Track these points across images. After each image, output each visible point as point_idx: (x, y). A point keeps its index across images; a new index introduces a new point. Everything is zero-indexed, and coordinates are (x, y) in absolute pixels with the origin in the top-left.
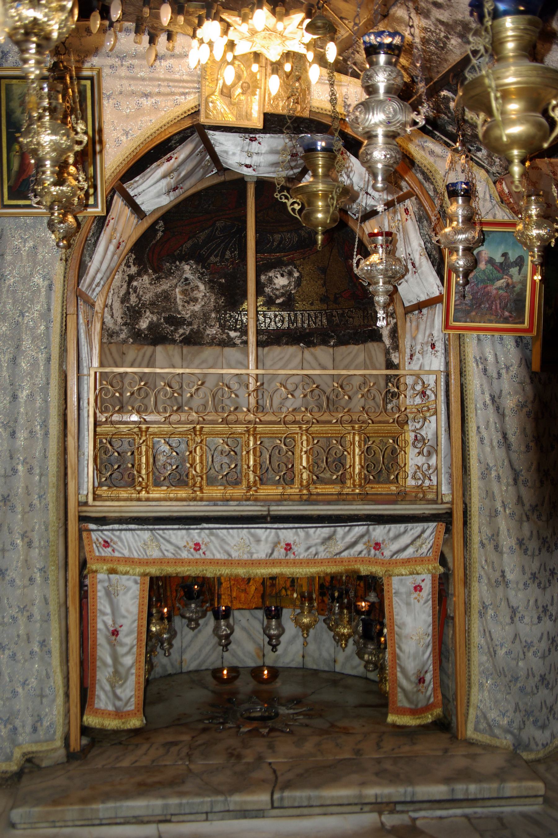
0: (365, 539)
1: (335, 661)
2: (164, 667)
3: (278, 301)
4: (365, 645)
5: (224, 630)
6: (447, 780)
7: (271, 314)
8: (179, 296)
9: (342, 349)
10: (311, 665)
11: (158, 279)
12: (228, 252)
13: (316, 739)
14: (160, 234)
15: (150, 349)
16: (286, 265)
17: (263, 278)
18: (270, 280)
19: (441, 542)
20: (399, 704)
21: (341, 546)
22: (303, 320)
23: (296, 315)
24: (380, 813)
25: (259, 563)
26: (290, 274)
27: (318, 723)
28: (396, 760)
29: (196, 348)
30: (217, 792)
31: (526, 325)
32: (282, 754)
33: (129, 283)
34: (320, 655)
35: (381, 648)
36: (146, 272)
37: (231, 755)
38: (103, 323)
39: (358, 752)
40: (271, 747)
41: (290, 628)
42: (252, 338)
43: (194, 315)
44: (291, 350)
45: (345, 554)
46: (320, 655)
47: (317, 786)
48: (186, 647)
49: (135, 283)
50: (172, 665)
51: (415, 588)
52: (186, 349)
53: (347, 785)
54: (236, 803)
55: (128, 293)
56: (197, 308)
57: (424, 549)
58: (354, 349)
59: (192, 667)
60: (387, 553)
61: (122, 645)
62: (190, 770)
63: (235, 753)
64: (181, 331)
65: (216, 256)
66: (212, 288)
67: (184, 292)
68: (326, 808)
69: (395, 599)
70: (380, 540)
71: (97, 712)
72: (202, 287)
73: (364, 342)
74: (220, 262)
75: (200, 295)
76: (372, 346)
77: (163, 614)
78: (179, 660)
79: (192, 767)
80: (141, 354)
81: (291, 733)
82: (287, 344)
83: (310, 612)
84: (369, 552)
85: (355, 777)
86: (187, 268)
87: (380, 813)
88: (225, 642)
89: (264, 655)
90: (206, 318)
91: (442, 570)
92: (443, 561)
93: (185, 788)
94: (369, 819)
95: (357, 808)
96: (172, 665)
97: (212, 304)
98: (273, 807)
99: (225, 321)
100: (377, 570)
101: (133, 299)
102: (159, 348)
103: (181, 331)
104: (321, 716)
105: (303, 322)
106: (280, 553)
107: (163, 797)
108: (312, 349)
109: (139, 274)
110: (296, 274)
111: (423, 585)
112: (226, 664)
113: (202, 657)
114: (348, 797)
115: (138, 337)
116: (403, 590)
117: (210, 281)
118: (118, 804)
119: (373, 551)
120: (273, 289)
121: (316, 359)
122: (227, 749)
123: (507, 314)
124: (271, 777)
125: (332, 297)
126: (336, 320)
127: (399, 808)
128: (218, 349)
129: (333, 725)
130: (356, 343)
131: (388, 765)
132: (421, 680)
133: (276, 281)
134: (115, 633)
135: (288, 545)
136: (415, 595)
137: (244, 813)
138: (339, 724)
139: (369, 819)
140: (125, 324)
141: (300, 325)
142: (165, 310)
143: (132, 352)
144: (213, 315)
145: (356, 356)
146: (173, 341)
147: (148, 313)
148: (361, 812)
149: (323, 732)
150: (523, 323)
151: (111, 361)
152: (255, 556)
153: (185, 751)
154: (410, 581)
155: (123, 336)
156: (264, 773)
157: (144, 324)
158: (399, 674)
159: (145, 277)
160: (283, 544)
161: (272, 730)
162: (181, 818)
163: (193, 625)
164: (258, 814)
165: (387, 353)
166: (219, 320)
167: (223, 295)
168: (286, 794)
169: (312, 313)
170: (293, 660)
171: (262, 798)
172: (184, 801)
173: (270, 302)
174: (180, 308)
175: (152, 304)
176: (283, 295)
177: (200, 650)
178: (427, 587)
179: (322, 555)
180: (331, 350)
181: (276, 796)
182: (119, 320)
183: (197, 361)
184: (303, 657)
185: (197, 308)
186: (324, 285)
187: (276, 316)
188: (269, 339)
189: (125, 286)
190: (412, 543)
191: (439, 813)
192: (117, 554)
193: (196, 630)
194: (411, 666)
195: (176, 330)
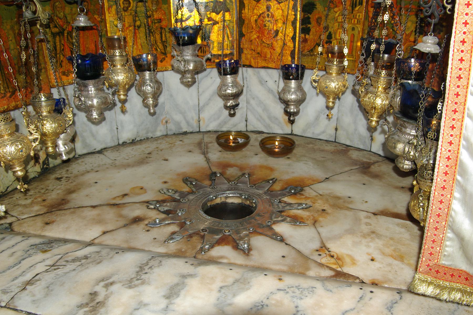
2: (178, 124)
10: (343, 140)
20: (444, 262)
34: (356, 130)
46: (356, 130)
48: (204, 106)
50: (188, 123)
63: (100, 298)
78: (196, 118)
96: (188, 123)
122: (103, 280)
129: (323, 248)
153: (40, 268)
158: (457, 206)
170: (324, 132)
184: (336, 129)
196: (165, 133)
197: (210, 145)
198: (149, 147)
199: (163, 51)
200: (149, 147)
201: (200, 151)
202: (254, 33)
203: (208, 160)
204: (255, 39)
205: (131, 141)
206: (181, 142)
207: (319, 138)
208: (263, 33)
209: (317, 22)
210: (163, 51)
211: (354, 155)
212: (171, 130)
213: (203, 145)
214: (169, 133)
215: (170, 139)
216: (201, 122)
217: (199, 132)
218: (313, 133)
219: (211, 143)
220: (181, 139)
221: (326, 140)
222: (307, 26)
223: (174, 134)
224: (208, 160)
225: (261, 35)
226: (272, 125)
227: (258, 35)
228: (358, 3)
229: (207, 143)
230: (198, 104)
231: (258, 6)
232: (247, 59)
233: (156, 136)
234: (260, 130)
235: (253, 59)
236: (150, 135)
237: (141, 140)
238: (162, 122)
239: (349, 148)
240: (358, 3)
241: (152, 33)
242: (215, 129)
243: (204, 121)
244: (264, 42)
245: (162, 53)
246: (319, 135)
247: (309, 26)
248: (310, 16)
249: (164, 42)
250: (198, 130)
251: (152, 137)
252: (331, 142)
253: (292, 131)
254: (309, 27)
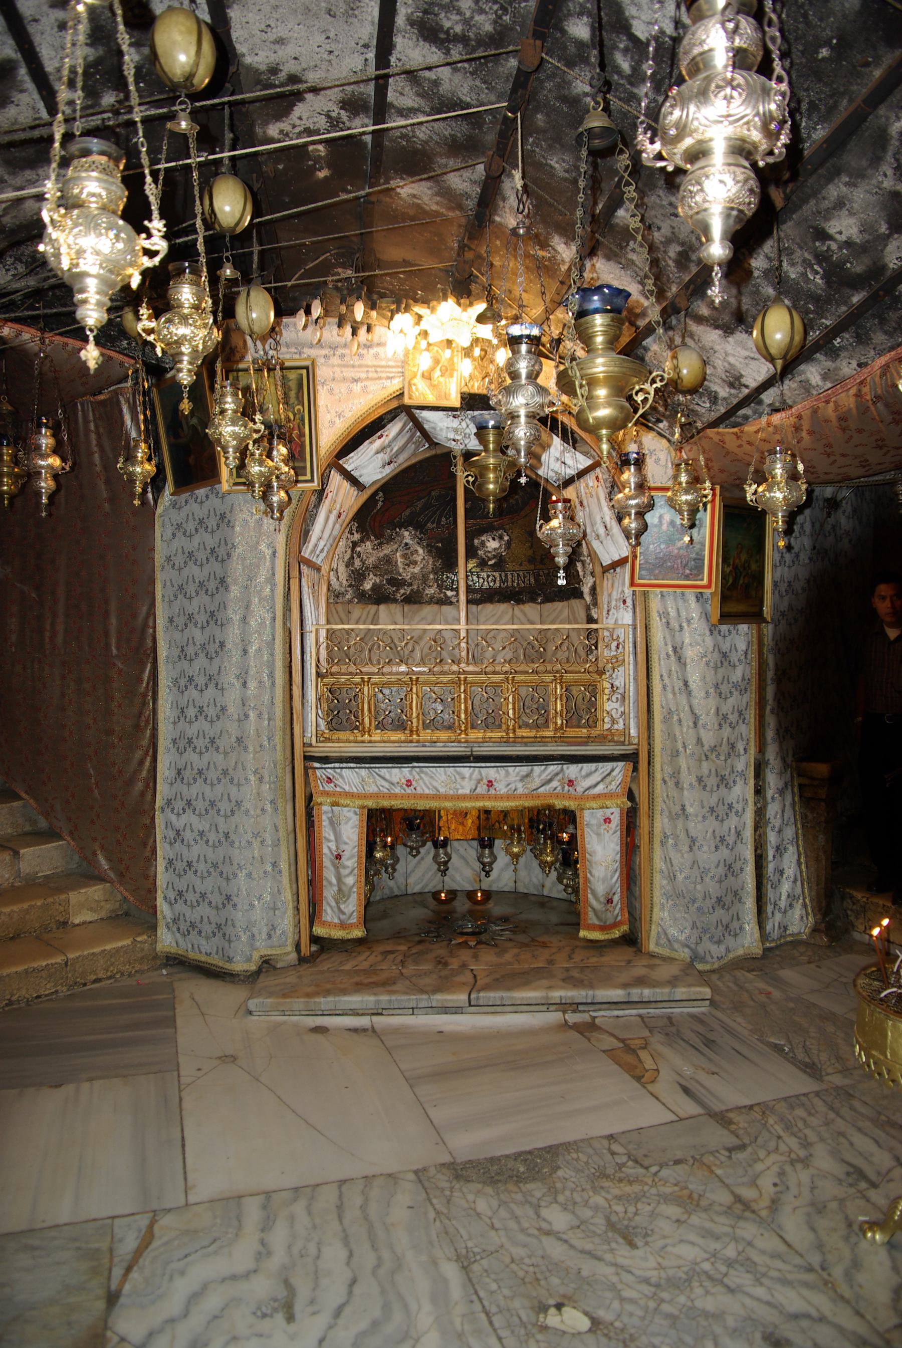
0: (560, 776)
2: (391, 889)
3: (490, 563)
4: (564, 871)
5: (443, 858)
6: (625, 986)
7: (484, 575)
8: (400, 560)
9: (549, 605)
10: (521, 889)
11: (380, 544)
12: (444, 519)
13: (516, 951)
14: (380, 504)
15: (374, 608)
16: (497, 530)
17: (476, 541)
18: (483, 544)
19: (629, 779)
21: (537, 782)
22: (513, 580)
23: (506, 576)
24: (564, 1012)
25: (464, 797)
26: (501, 538)
27: (522, 938)
28: (582, 969)
29: (416, 606)
30: (422, 991)
31: (705, 582)
32: (485, 961)
33: (353, 549)
35: (576, 874)
36: (368, 539)
37: (440, 962)
38: (329, 585)
39: (551, 962)
40: (476, 957)
41: (502, 859)
42: (463, 597)
43: (414, 576)
44: (503, 607)
45: (542, 790)
47: (509, 989)
49: (358, 549)
50: (398, 887)
51: (605, 821)
52: (406, 608)
53: (535, 989)
54: (438, 1001)
55: (352, 558)
56: (417, 570)
57: (613, 786)
58: (558, 605)
59: (417, 889)
60: (580, 789)
61: (344, 867)
62: (402, 974)
64: (402, 591)
65: (433, 523)
66: (430, 552)
67: (404, 556)
68: (517, 1007)
69: (587, 830)
70: (573, 777)
71: (324, 924)
72: (421, 551)
73: (568, 599)
74: (437, 527)
75: (419, 559)
76: (575, 602)
77: (386, 842)
79: (404, 971)
80: (365, 612)
81: (496, 945)
82: (499, 602)
83: (519, 842)
84: (563, 788)
85: (545, 982)
86: (406, 534)
87: (564, 1012)
88: (443, 868)
90: (425, 579)
91: (629, 804)
92: (631, 796)
93: (395, 988)
94: (555, 1017)
95: (544, 1008)
96: (398, 887)
97: (430, 566)
98: (470, 1005)
99: (443, 582)
100: (571, 805)
101: (357, 563)
102: (382, 607)
103: (402, 591)
104: (524, 932)
105: (513, 581)
106: (482, 789)
107: (375, 994)
108: (521, 606)
109: (362, 540)
110: (506, 538)
111: (612, 817)
112: (446, 888)
114: (536, 998)
115: (363, 597)
116: (594, 822)
117: (428, 545)
118: (337, 999)
119: (566, 788)
120: (486, 552)
121: (525, 615)
123: (688, 571)
124: (472, 980)
125: (538, 558)
126: (543, 579)
127: (581, 1008)
128: (436, 607)
129: (533, 940)
130: (561, 600)
131: (575, 974)
132: (610, 901)
133: (488, 544)
134: (339, 857)
135: (490, 781)
136: (605, 826)
137: (445, 1010)
138: (539, 939)
139: (555, 1017)
140: (350, 586)
141: (510, 584)
142: (387, 572)
143: (357, 610)
144: (432, 576)
145: (561, 612)
146: (395, 601)
147: (371, 576)
148: (548, 1010)
149: (524, 945)
150: (702, 580)
151: (337, 619)
152: (460, 792)
153: (400, 958)
154: (600, 814)
155: (348, 596)
156: (467, 977)
157: (368, 586)
158: (590, 896)
159: (368, 543)
160: (485, 781)
161: (479, 943)
162: (391, 1012)
163: (414, 852)
164: (458, 1010)
165: (588, 608)
166: (436, 580)
167: (440, 558)
168: (482, 994)
169: (521, 573)
171: (461, 998)
172: (393, 998)
173: (483, 564)
174: (401, 570)
175: (375, 567)
176: (495, 557)
177: (423, 875)
178: (616, 819)
179: (520, 791)
180: (538, 607)
181: (473, 996)
182: (345, 582)
183: (417, 619)
185: (417, 570)
186: (531, 547)
187: (488, 576)
188: (480, 597)
189: (349, 552)
190: (602, 780)
191: (616, 1013)
192: (338, 789)
193: (418, 858)
194: (601, 889)
195: (398, 590)
211: (533, 898)
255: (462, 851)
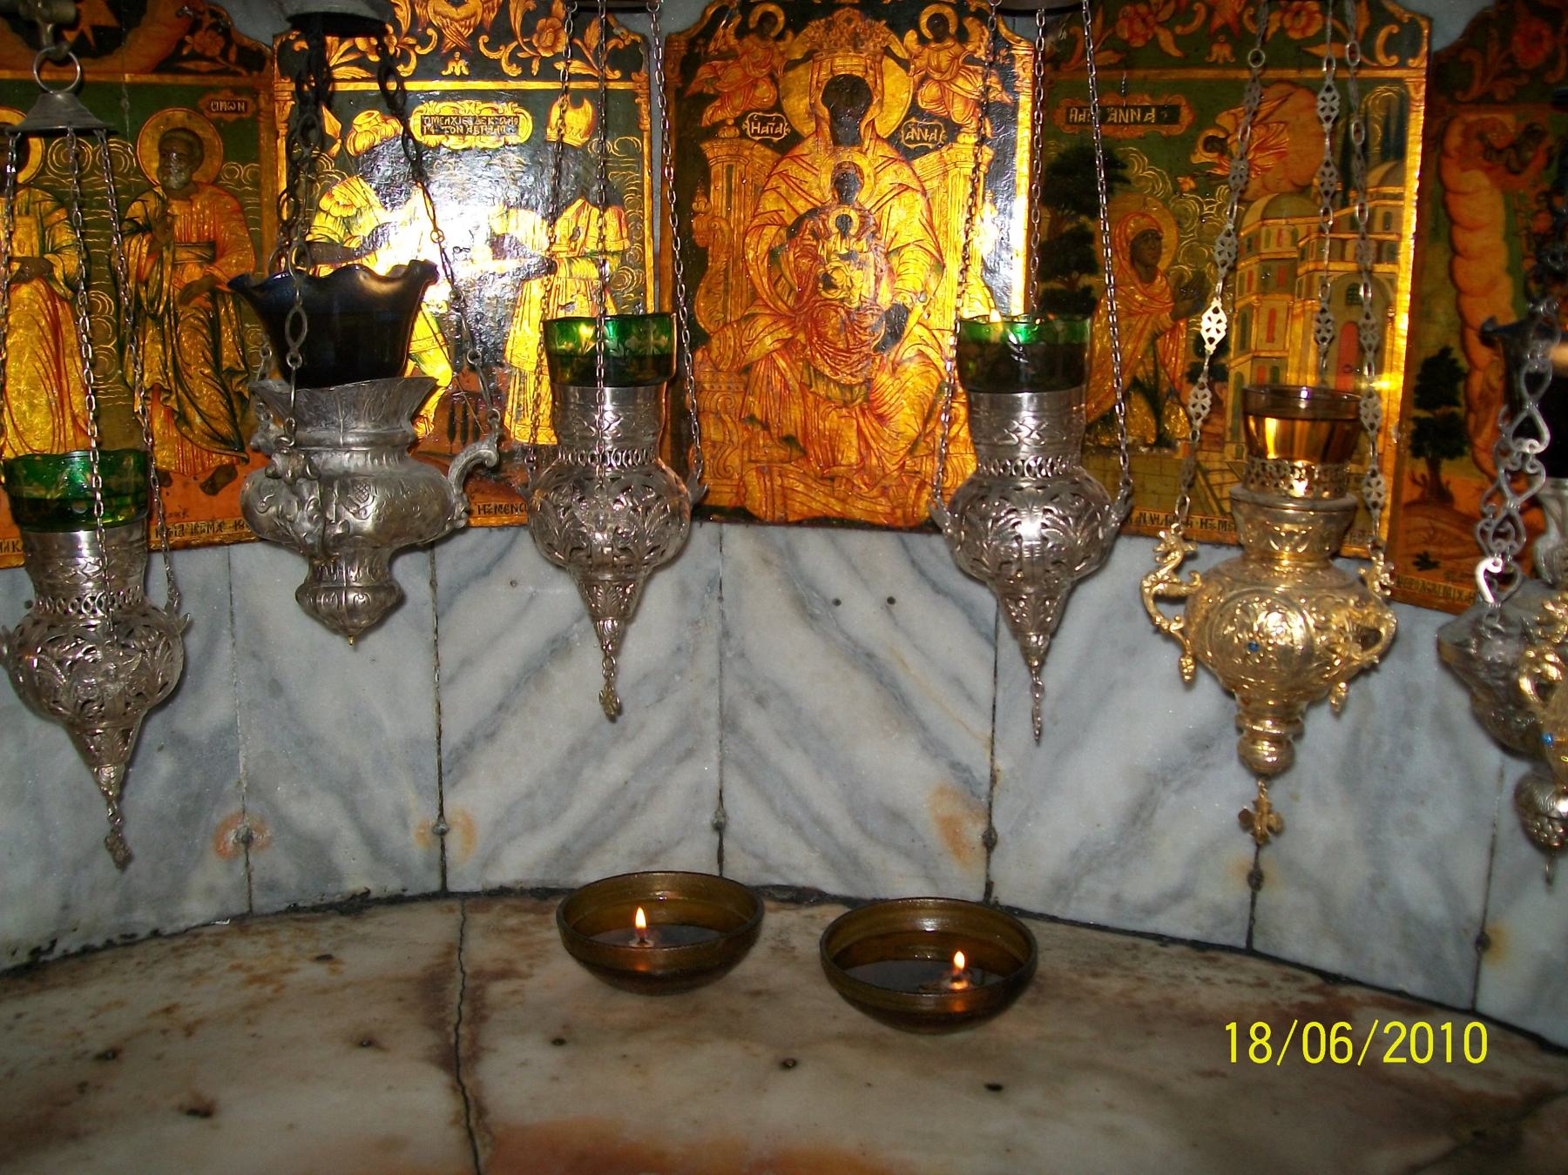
1: (1483, 942)
2: (315, 851)
10: (1298, 938)
34: (1378, 883)
46: (1378, 883)
50: (373, 842)
78: (422, 813)
89: (990, 841)
96: (373, 842)
113: (581, 808)
170: (1179, 895)
196: (237, 906)
197: (497, 990)
198: (120, 1004)
199: (225, 429)
200: (120, 1004)
201: (431, 1039)
202: (762, 322)
203: (472, 1112)
204: (768, 357)
205: (23, 958)
206: (320, 971)
207: (1149, 926)
208: (816, 322)
209: (1135, 259)
210: (225, 429)
212: (271, 886)
213: (454, 990)
214: (262, 902)
215: (263, 940)
216: (454, 842)
217: (443, 894)
218: (1116, 899)
219: (502, 975)
220: (325, 947)
221: (1197, 945)
222: (1072, 284)
223: (294, 909)
224: (472, 1112)
225: (801, 337)
226: (871, 854)
227: (785, 334)
228: (1375, 149)
229: (479, 974)
230: (430, 732)
231: (785, 176)
232: (722, 472)
233: (182, 925)
234: (799, 880)
235: (760, 471)
236: (144, 918)
237: (87, 951)
238: (219, 837)
239: (1344, 991)
240: (1375, 149)
241: (158, 320)
242: (536, 877)
243: (469, 830)
244: (819, 374)
245: (216, 437)
246: (1149, 910)
247: (1086, 280)
248: (1091, 225)
249: (232, 372)
250: (434, 884)
251: (156, 934)
252: (1227, 958)
253: (989, 886)
254: (1088, 289)
255: (861, 615)
